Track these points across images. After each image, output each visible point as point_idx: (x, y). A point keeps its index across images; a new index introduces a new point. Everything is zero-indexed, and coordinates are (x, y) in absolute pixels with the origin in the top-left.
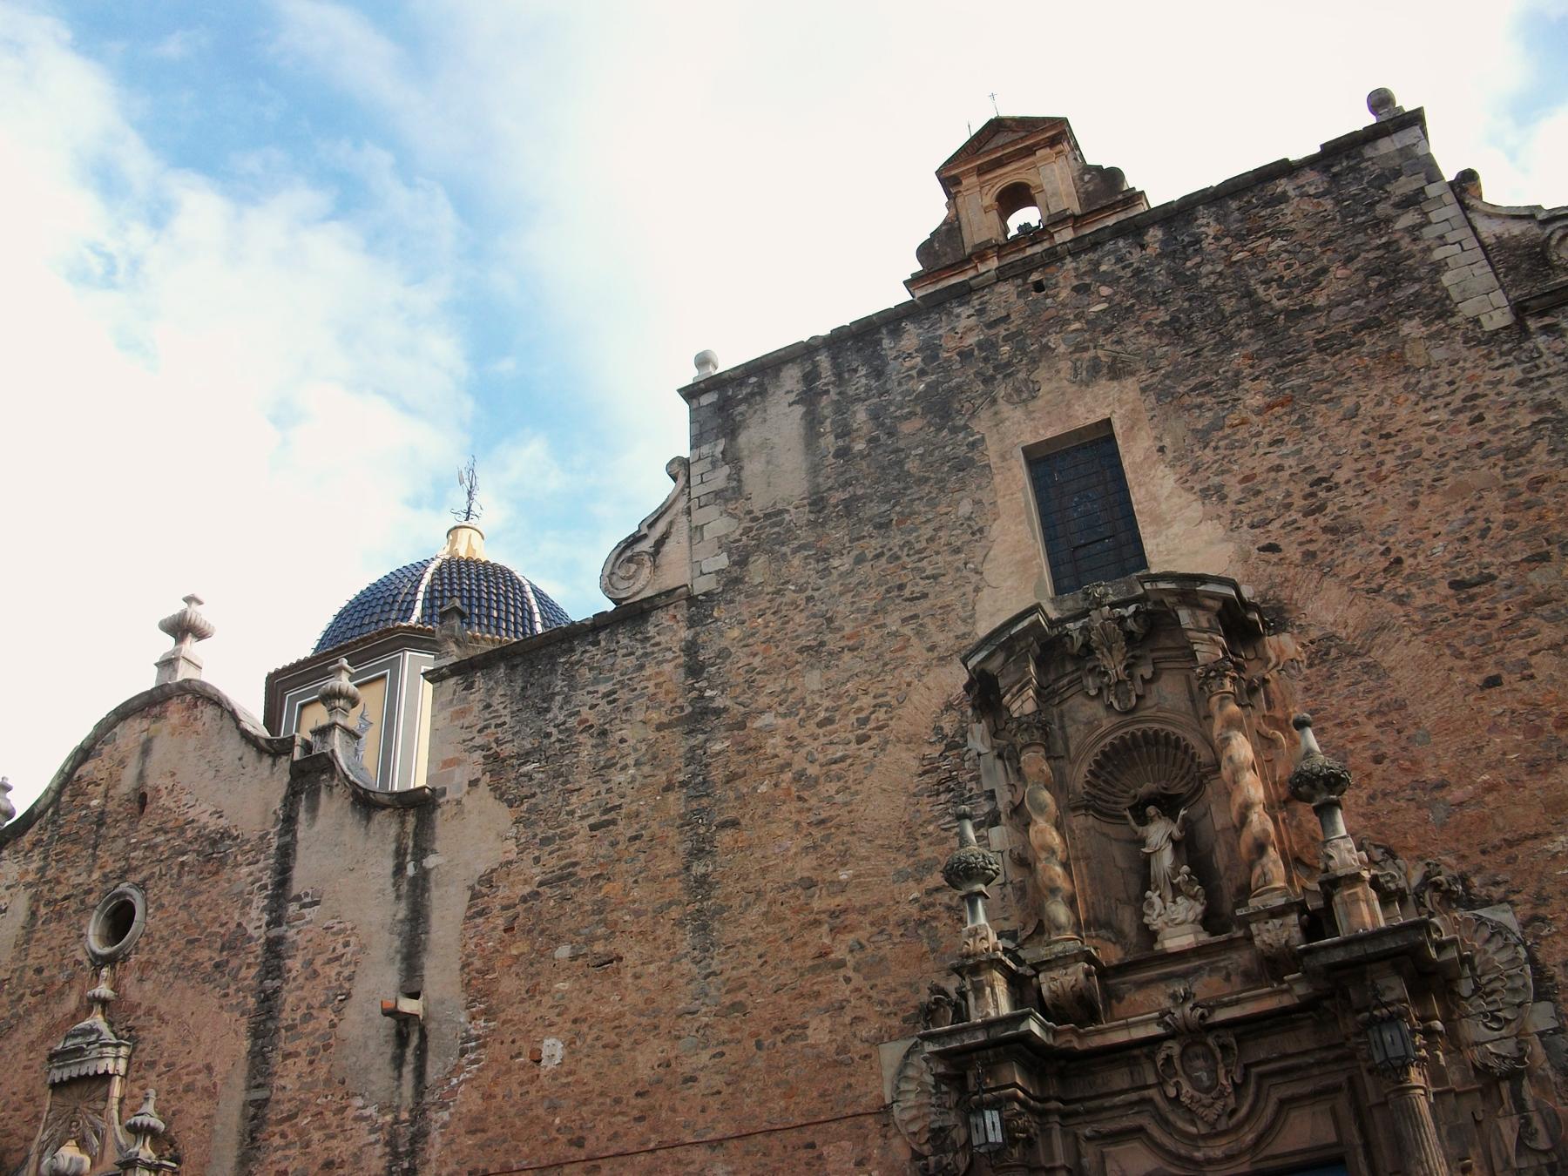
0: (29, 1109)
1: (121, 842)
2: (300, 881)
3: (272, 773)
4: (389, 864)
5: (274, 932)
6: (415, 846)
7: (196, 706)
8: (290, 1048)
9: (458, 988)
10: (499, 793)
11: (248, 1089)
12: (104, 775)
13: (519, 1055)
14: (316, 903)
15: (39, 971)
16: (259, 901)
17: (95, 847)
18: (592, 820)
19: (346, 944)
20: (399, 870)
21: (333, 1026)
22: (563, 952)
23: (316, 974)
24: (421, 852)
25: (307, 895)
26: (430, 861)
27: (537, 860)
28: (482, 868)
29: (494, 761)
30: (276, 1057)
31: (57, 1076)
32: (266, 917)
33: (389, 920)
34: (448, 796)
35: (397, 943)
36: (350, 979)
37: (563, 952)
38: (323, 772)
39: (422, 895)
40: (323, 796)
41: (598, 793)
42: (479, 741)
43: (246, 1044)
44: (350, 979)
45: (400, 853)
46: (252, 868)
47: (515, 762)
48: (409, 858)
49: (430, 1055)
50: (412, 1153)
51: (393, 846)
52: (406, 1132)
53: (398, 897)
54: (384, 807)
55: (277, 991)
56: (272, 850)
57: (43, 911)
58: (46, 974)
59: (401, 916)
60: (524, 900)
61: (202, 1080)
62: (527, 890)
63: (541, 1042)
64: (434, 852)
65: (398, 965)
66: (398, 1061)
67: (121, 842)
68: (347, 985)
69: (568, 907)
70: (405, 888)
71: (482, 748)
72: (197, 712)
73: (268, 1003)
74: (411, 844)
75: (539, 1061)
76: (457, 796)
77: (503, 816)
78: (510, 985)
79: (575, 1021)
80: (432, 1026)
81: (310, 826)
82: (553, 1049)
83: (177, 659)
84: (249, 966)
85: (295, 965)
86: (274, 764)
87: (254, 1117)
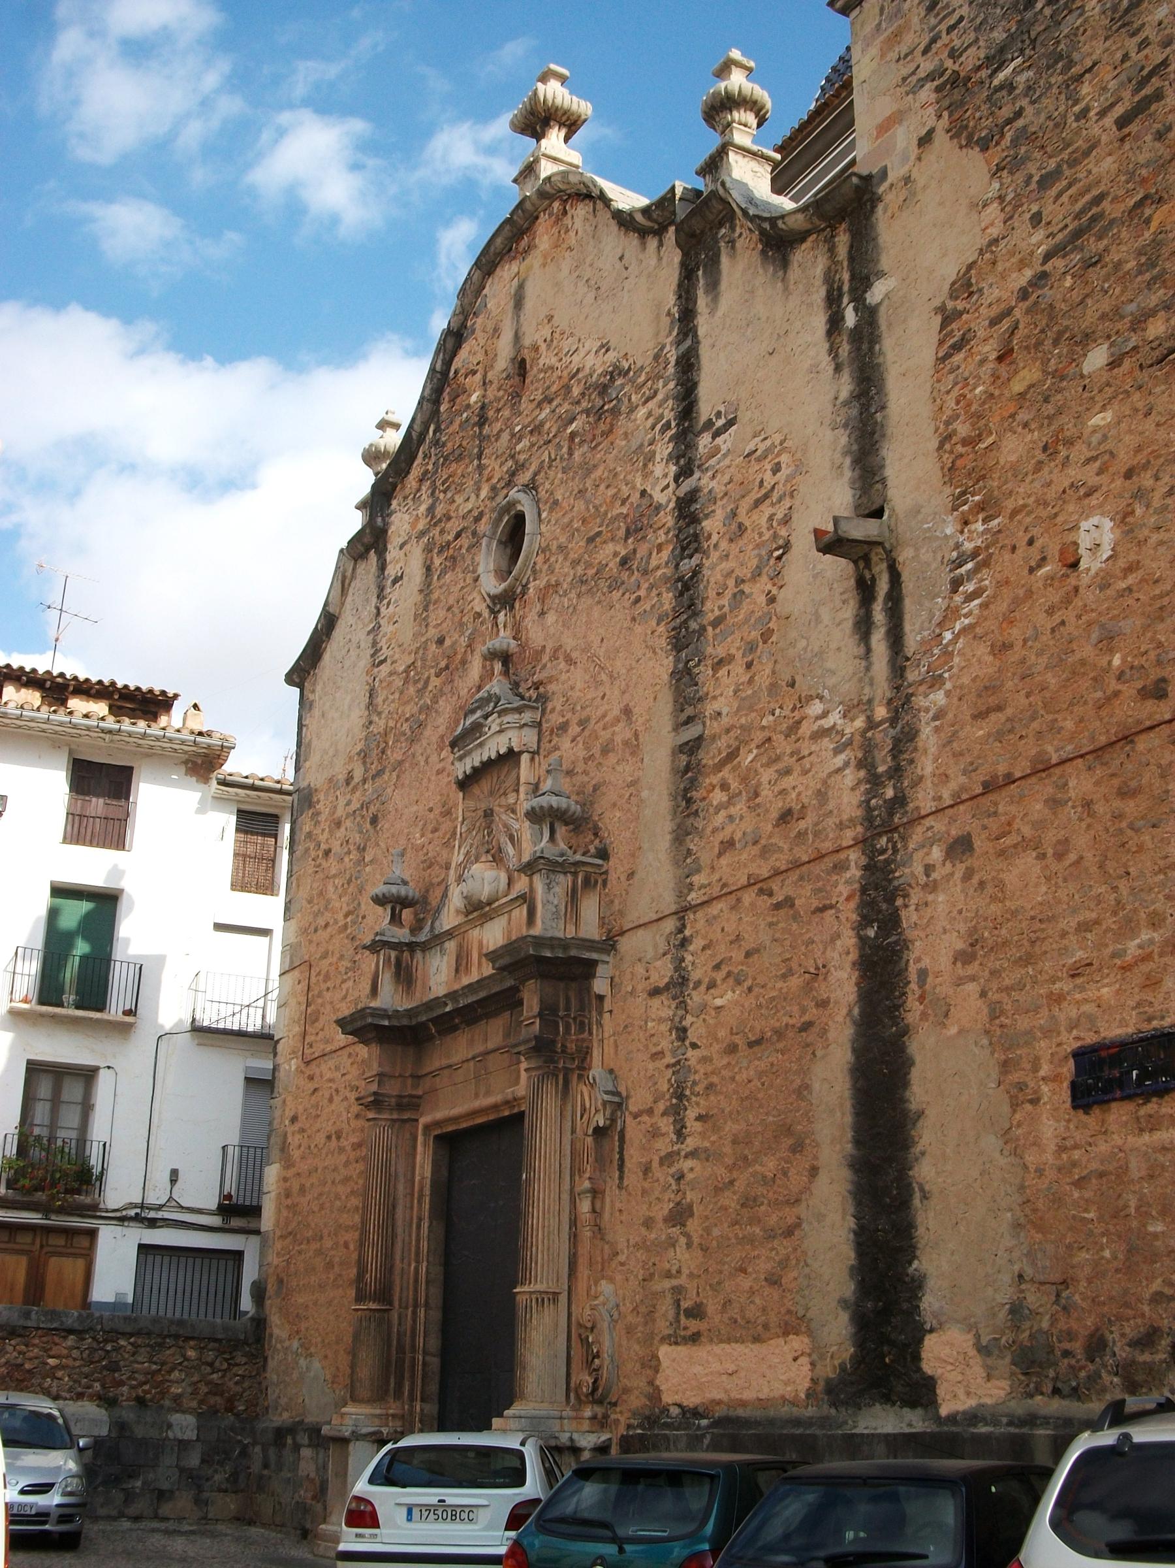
0: (446, 826)
1: (505, 436)
2: (710, 401)
3: (660, 259)
4: (820, 322)
5: (687, 485)
6: (853, 278)
7: (565, 212)
8: (721, 652)
9: (936, 477)
10: (963, 135)
11: (678, 727)
12: (480, 357)
13: (1043, 560)
14: (731, 423)
15: (440, 641)
16: (664, 449)
17: (479, 457)
18: (1119, 110)
19: (776, 469)
20: (835, 322)
21: (772, 600)
22: (1096, 358)
23: (741, 528)
24: (862, 282)
25: (719, 415)
26: (877, 293)
27: (1036, 220)
28: (950, 270)
29: (953, 88)
30: (704, 672)
31: (463, 768)
32: (673, 469)
33: (830, 408)
34: (892, 177)
35: (844, 440)
36: (786, 520)
37: (1096, 358)
38: (721, 225)
39: (871, 349)
40: (725, 260)
41: (1126, 58)
42: (927, 66)
43: (668, 662)
44: (786, 520)
45: (833, 300)
46: (650, 405)
47: (984, 73)
48: (845, 300)
49: (908, 605)
50: (896, 772)
51: (823, 292)
52: (884, 738)
53: (838, 369)
54: (802, 237)
55: (696, 572)
56: (671, 370)
57: (437, 561)
58: (448, 642)
59: (844, 394)
60: (1024, 294)
61: (622, 733)
62: (1028, 273)
63: (1075, 528)
64: (881, 274)
65: (848, 474)
66: (863, 626)
67: (505, 436)
68: (783, 532)
69: (1094, 274)
70: (845, 349)
71: (931, 77)
72: (567, 221)
73: (687, 588)
74: (846, 276)
75: (1075, 565)
76: (903, 171)
77: (975, 170)
78: (1014, 448)
79: (1128, 475)
80: (904, 555)
81: (712, 312)
82: (1097, 534)
83: (536, 161)
84: (660, 548)
85: (712, 525)
86: (661, 244)
87: (688, 768)
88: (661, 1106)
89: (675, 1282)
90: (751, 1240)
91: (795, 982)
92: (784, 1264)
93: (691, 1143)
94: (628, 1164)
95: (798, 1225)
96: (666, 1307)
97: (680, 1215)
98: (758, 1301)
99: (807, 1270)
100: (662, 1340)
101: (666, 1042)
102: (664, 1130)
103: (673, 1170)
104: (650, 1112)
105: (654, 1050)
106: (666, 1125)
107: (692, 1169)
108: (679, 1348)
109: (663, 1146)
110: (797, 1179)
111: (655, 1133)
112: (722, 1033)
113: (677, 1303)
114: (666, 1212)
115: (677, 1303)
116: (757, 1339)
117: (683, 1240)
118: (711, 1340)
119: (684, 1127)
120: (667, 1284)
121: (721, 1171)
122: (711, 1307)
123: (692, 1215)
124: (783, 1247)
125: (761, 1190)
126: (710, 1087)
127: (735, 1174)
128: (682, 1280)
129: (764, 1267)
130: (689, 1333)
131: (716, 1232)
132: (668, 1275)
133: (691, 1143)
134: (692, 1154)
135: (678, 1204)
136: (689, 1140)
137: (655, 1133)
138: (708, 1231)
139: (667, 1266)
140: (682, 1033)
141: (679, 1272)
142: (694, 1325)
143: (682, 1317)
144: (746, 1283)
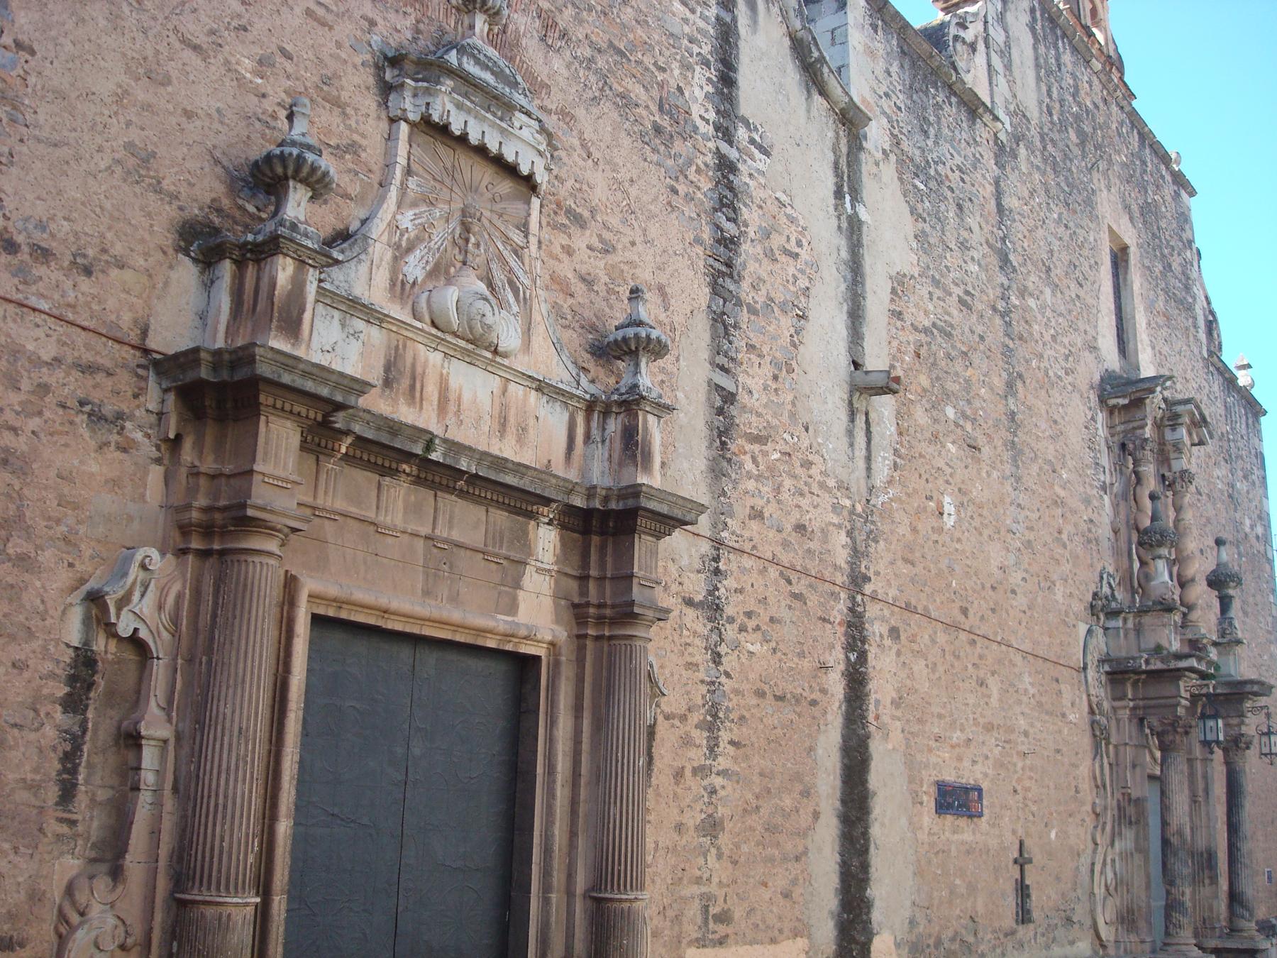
66: (850, 433)
88: (695, 717)
89: (704, 889)
90: (771, 860)
91: (806, 664)
92: (794, 882)
93: (722, 763)
94: (658, 764)
95: (805, 852)
96: (694, 910)
97: (712, 827)
98: (775, 910)
99: (811, 889)
100: (690, 944)
101: (701, 657)
102: (698, 742)
103: (705, 782)
104: (683, 718)
105: (689, 660)
106: (700, 737)
107: (723, 787)
108: (706, 950)
109: (697, 756)
110: (805, 819)
111: (687, 742)
112: (752, 676)
113: (706, 909)
114: (698, 821)
115: (706, 909)
116: (773, 941)
117: (713, 851)
118: (737, 943)
119: (717, 745)
120: (696, 890)
121: (750, 796)
122: (738, 913)
123: (723, 829)
124: (795, 868)
125: (779, 820)
126: (742, 718)
127: (760, 803)
128: (713, 888)
129: (781, 883)
130: (717, 936)
131: (745, 848)
132: (698, 881)
133: (722, 763)
134: (723, 773)
135: (710, 816)
136: (720, 759)
137: (687, 742)
138: (737, 846)
139: (698, 873)
140: (717, 658)
141: (709, 880)
142: (722, 929)
143: (711, 925)
144: (766, 894)
